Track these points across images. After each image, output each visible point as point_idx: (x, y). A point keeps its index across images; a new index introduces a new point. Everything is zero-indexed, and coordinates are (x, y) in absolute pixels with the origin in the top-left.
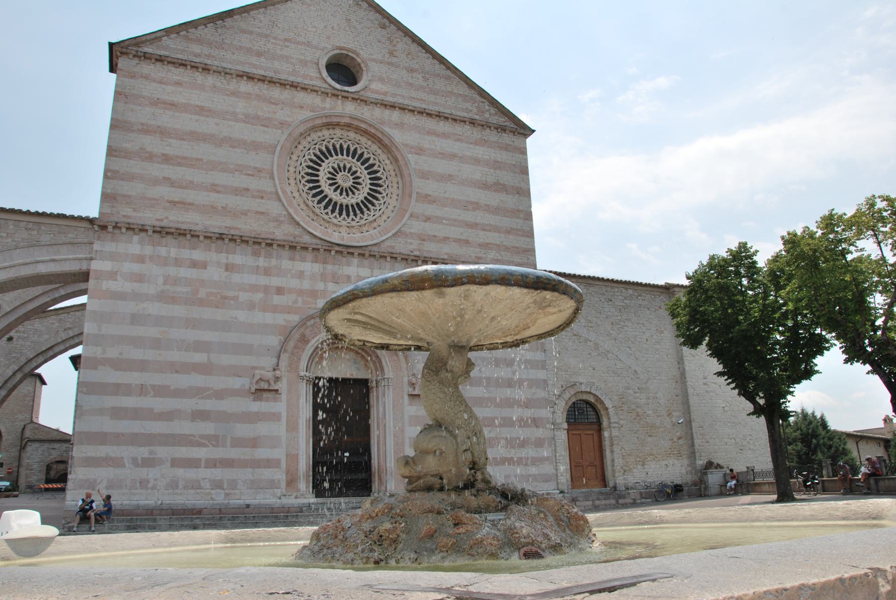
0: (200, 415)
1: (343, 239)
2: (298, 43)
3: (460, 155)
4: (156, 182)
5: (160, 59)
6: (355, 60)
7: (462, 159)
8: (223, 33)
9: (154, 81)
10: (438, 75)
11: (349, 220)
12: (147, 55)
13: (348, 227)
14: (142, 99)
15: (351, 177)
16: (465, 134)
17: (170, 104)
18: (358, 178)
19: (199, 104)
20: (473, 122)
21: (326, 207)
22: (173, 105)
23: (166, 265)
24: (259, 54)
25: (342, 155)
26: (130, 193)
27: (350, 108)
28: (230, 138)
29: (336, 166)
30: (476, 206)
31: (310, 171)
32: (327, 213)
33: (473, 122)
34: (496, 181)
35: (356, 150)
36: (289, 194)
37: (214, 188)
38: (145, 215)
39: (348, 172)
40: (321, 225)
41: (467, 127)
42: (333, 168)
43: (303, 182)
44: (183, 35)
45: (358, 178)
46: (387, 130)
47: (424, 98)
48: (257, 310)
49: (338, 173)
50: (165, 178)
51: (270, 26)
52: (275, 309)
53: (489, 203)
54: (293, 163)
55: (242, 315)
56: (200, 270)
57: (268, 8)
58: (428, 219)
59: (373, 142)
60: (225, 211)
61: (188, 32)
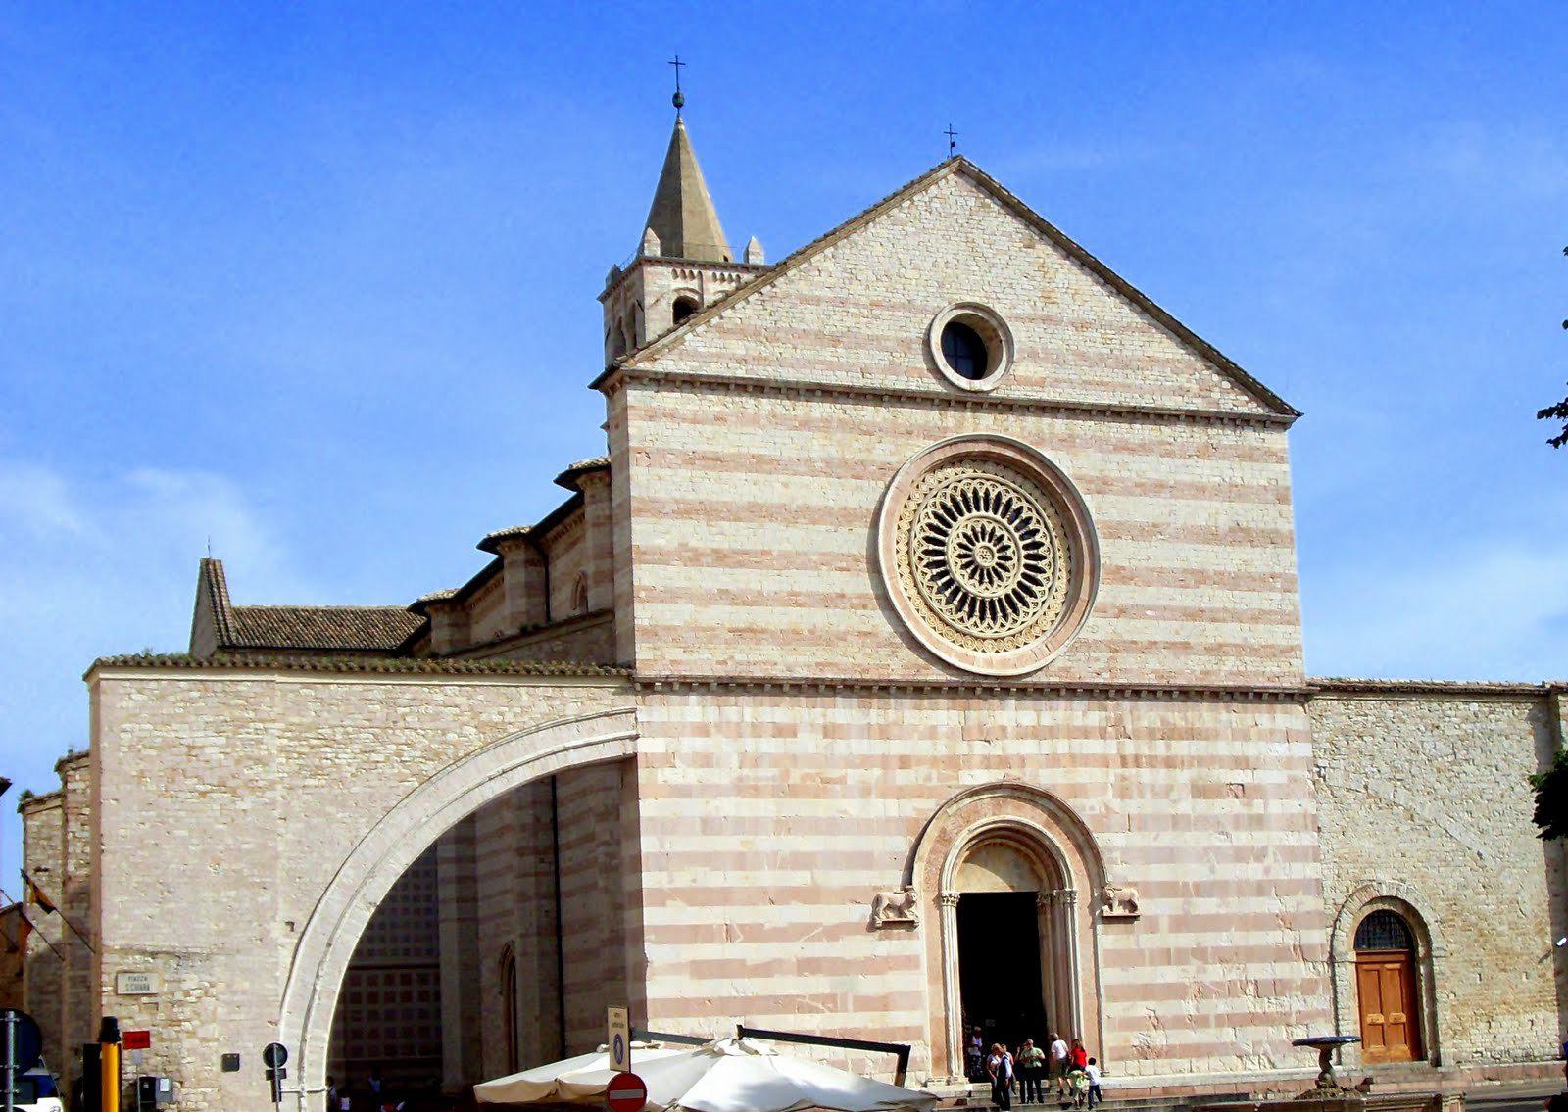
1: (990, 663)
2: (893, 307)
3: (1172, 483)
4: (710, 598)
6: (987, 321)
7: (1174, 489)
8: (775, 309)
9: (684, 420)
10: (1129, 325)
11: (996, 627)
12: (670, 378)
13: (995, 640)
14: (672, 456)
15: (994, 549)
16: (1179, 440)
17: (713, 459)
18: (1007, 547)
19: (754, 451)
21: (959, 609)
22: (717, 459)
23: (740, 735)
24: (835, 341)
25: (978, 509)
26: (676, 623)
27: (986, 424)
28: (808, 508)
29: (970, 533)
30: (1201, 577)
31: (931, 547)
32: (962, 620)
34: (1234, 525)
35: (999, 496)
36: (903, 591)
37: (794, 599)
38: (701, 657)
39: (990, 541)
40: (954, 642)
42: (965, 536)
43: (921, 568)
44: (716, 326)
45: (1006, 548)
46: (1048, 454)
47: (1106, 380)
48: (873, 796)
49: (978, 540)
50: (724, 592)
51: (847, 282)
52: (901, 793)
53: (1222, 569)
54: (904, 539)
55: (853, 807)
56: (788, 739)
57: (839, 244)
58: (1122, 612)
59: (1025, 478)
60: (815, 637)
61: (722, 318)
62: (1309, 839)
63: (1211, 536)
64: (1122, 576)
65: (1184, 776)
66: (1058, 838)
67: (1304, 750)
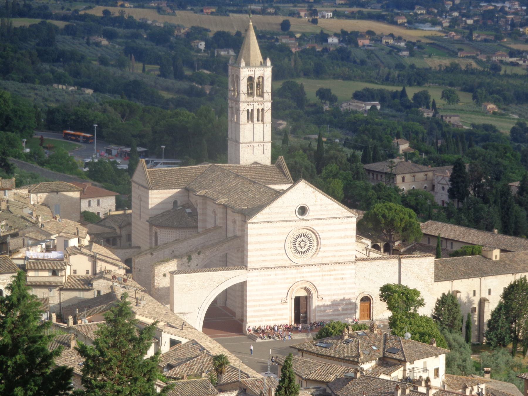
0: (271, 310)
5: (258, 223)
20: (339, 218)
24: (281, 213)
27: (304, 224)
30: (338, 244)
33: (339, 218)
37: (272, 255)
41: (338, 219)
50: (261, 255)
62: (353, 285)
63: (341, 237)
64: (325, 246)
65: (332, 277)
66: (311, 289)
67: (354, 271)
